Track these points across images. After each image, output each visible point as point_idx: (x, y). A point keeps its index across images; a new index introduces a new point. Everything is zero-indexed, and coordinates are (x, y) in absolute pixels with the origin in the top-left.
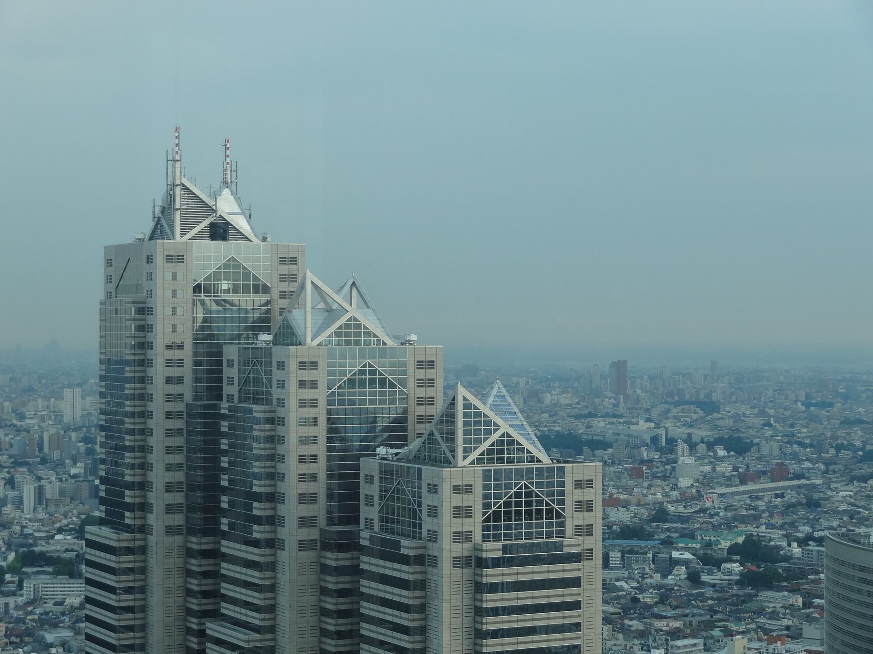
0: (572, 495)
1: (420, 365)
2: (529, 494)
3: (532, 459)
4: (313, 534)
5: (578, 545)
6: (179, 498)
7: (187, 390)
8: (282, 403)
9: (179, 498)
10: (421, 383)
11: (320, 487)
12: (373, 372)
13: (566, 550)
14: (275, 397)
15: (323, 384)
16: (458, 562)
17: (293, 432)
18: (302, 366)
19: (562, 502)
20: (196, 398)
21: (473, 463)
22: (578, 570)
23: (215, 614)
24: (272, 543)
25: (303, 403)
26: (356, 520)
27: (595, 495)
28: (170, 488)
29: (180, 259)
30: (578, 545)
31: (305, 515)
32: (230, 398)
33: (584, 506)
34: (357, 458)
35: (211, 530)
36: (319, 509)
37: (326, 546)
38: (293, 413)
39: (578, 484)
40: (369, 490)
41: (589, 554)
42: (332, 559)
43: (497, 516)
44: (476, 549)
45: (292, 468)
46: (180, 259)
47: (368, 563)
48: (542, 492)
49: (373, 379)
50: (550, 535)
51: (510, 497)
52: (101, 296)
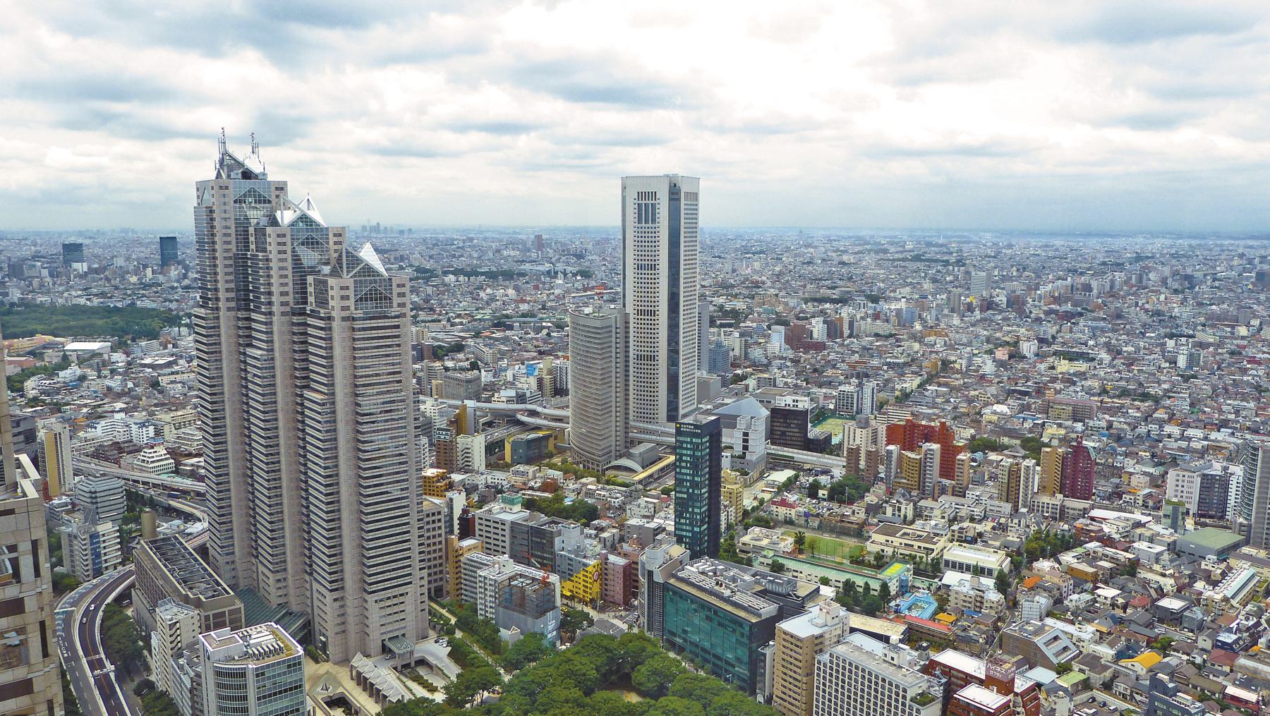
0: (396, 290)
1: (335, 235)
4: (288, 309)
6: (232, 295)
9: (232, 295)
11: (290, 289)
16: (344, 319)
24: (270, 313)
26: (306, 303)
27: (406, 290)
33: (402, 295)
36: (290, 299)
37: (294, 314)
39: (398, 286)
40: (311, 289)
41: (404, 315)
42: (295, 319)
43: (361, 299)
47: (310, 321)
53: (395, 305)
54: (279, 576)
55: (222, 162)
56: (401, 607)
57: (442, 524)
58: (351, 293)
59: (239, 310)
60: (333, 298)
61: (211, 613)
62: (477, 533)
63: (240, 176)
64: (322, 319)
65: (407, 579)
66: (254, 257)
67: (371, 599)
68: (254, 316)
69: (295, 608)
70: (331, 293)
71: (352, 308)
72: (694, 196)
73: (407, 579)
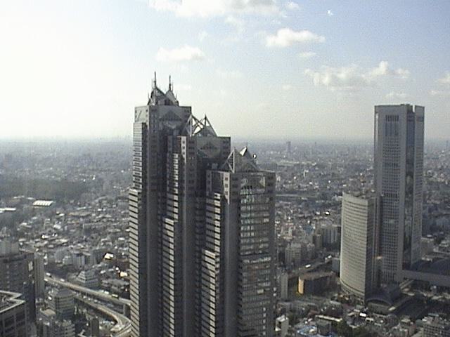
6: (155, 181)
9: (155, 181)
32: (170, 152)
35: (164, 190)
49: (210, 146)
52: (134, 121)
63: (164, 103)
72: (422, 119)
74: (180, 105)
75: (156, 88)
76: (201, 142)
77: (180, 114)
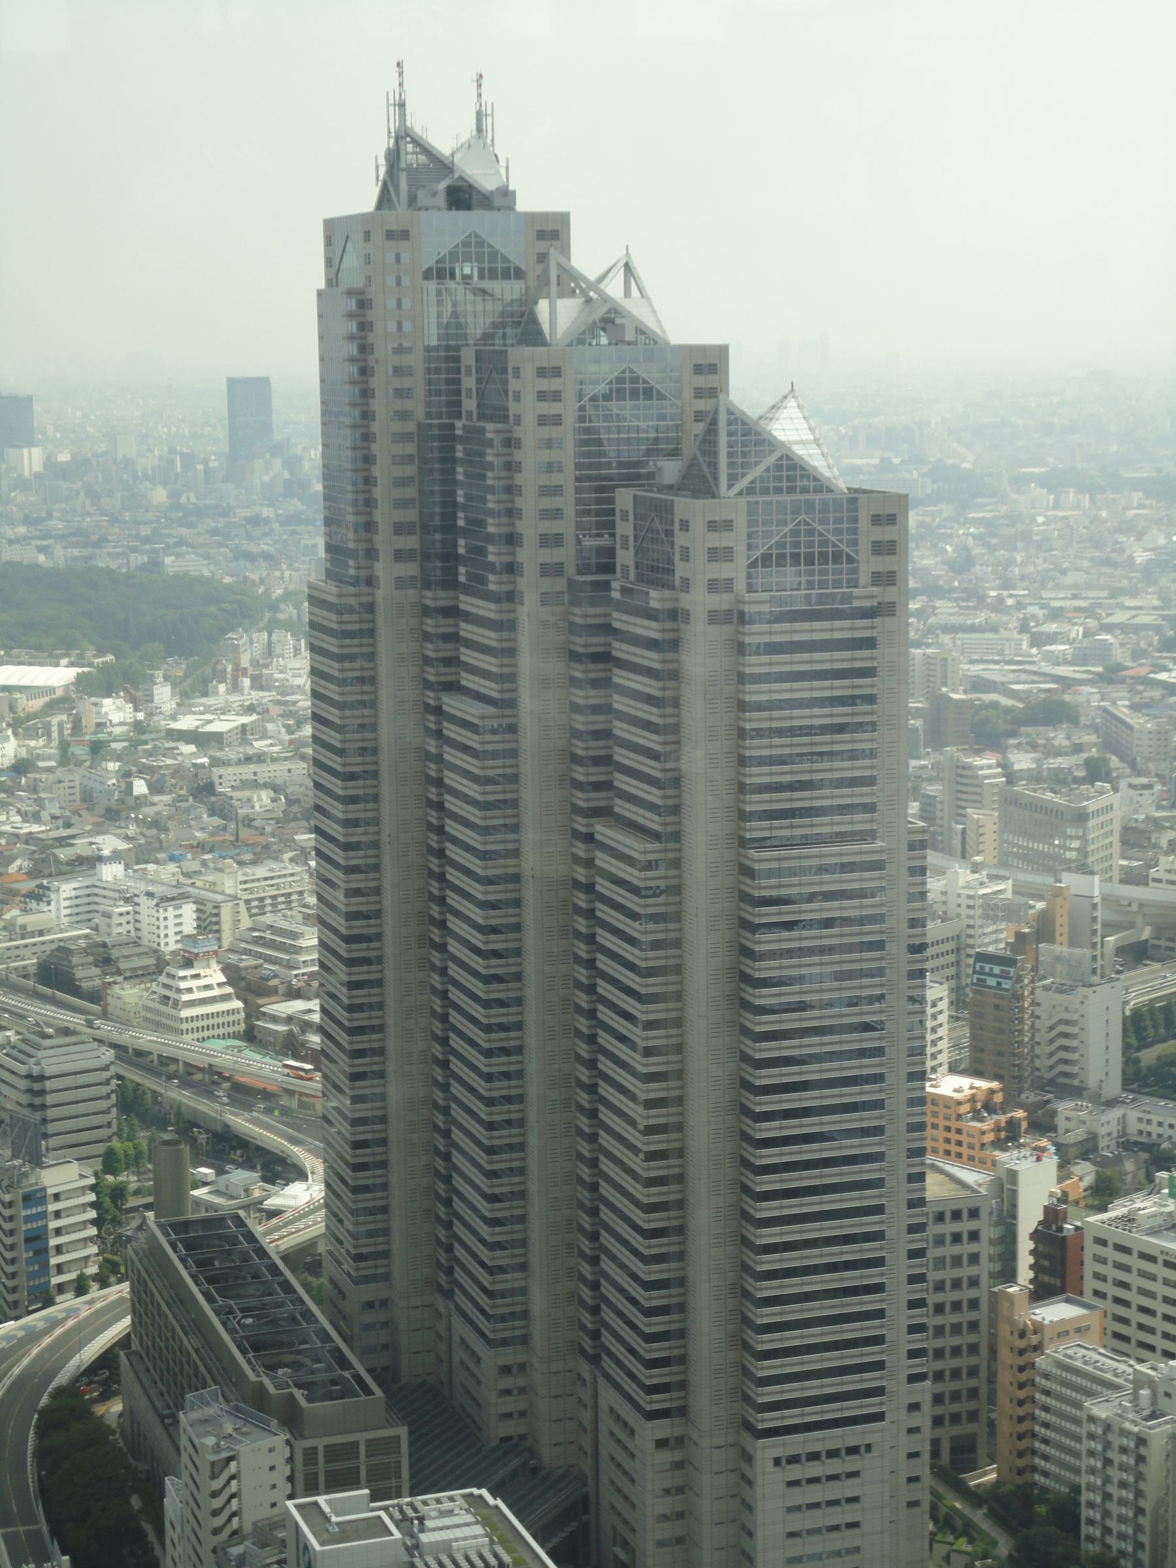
1: (698, 369)
2: (811, 532)
3: (830, 490)
5: (873, 597)
6: (411, 542)
7: (417, 406)
8: (518, 420)
9: (411, 542)
10: (699, 393)
12: (635, 380)
13: (856, 604)
14: (511, 413)
15: (569, 395)
16: (714, 617)
17: (530, 456)
18: (542, 372)
19: (854, 543)
20: (429, 415)
21: (740, 494)
22: (873, 628)
23: (453, 687)
25: (543, 420)
28: (399, 529)
29: (405, 235)
30: (873, 597)
31: (548, 561)
34: (612, 489)
36: (566, 555)
38: (529, 433)
39: (877, 520)
43: (766, 559)
44: (739, 601)
45: (529, 502)
46: (405, 235)
48: (828, 530)
49: (632, 388)
50: (837, 584)
51: (784, 536)
53: (864, 576)
54: (508, 1356)
55: (394, 157)
56: (849, 1488)
57: (984, 1248)
58: (736, 540)
59: (427, 584)
60: (686, 554)
61: (320, 1443)
62: (1089, 1284)
63: (441, 200)
64: (651, 615)
65: (870, 1406)
66: (474, 435)
67: (766, 1450)
68: (467, 603)
69: (550, 1455)
70: (680, 539)
71: (740, 585)
73: (870, 1406)
74: (524, 204)
75: (403, 136)
76: (599, 367)
77: (516, 250)
